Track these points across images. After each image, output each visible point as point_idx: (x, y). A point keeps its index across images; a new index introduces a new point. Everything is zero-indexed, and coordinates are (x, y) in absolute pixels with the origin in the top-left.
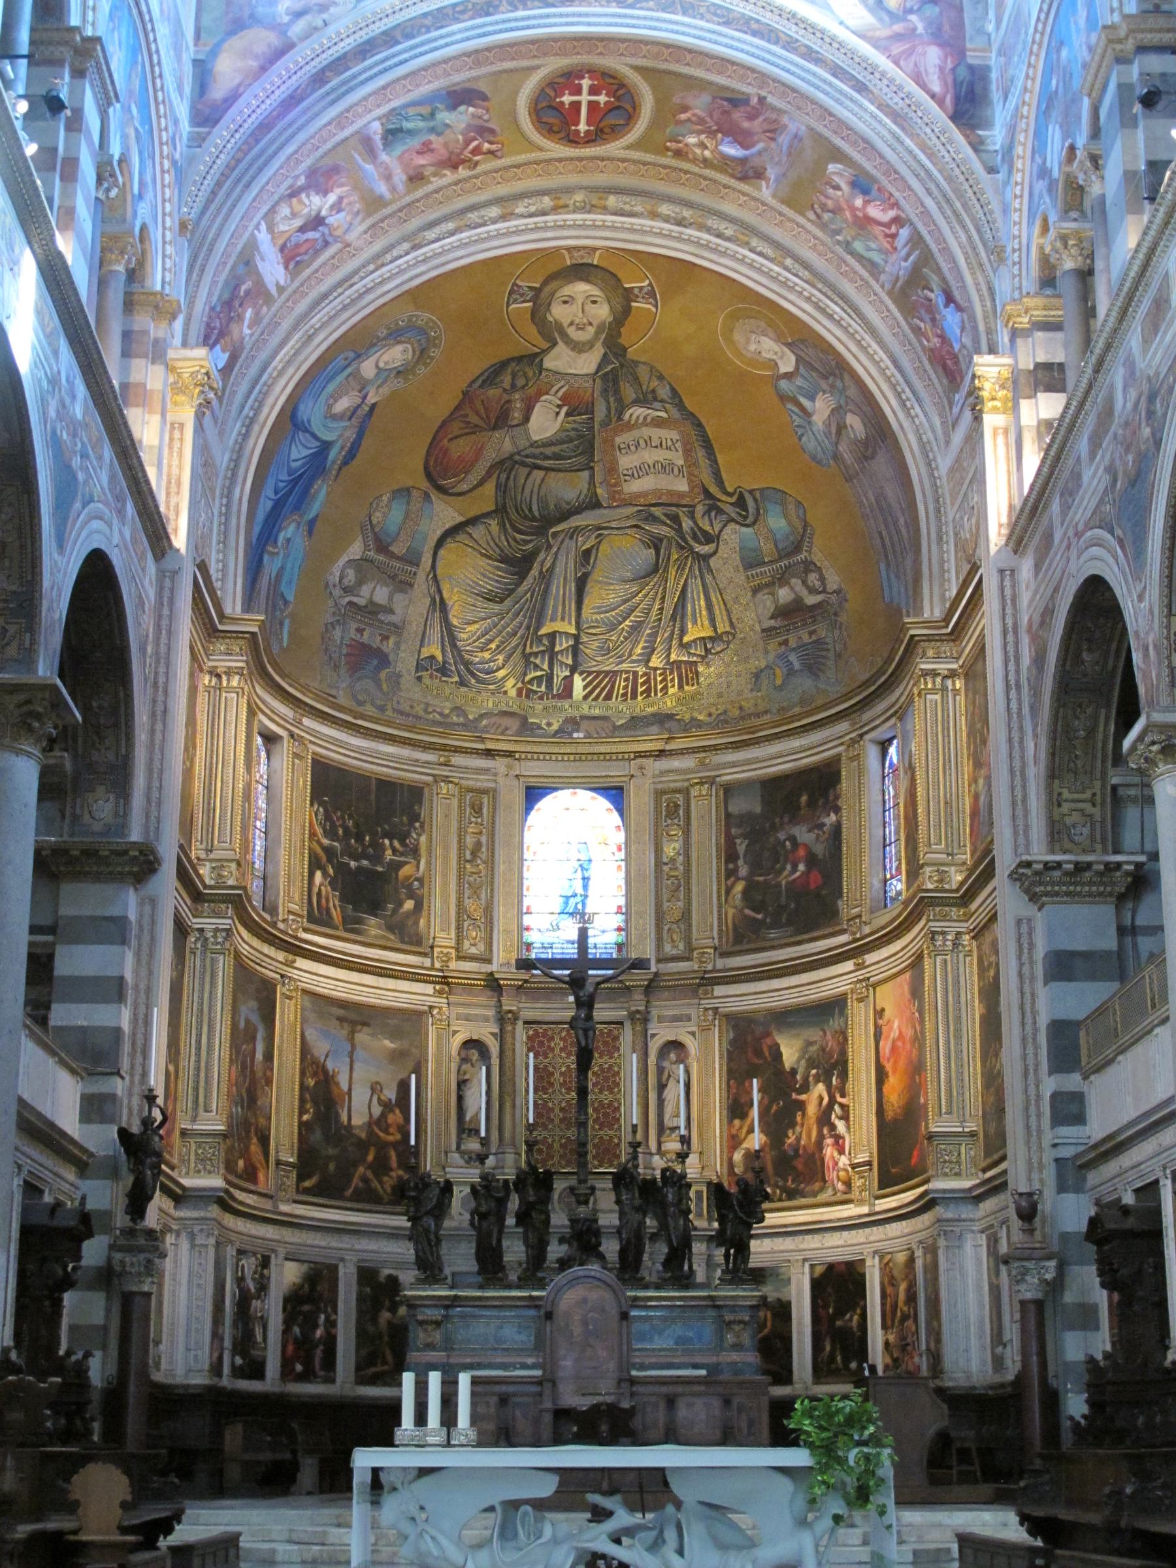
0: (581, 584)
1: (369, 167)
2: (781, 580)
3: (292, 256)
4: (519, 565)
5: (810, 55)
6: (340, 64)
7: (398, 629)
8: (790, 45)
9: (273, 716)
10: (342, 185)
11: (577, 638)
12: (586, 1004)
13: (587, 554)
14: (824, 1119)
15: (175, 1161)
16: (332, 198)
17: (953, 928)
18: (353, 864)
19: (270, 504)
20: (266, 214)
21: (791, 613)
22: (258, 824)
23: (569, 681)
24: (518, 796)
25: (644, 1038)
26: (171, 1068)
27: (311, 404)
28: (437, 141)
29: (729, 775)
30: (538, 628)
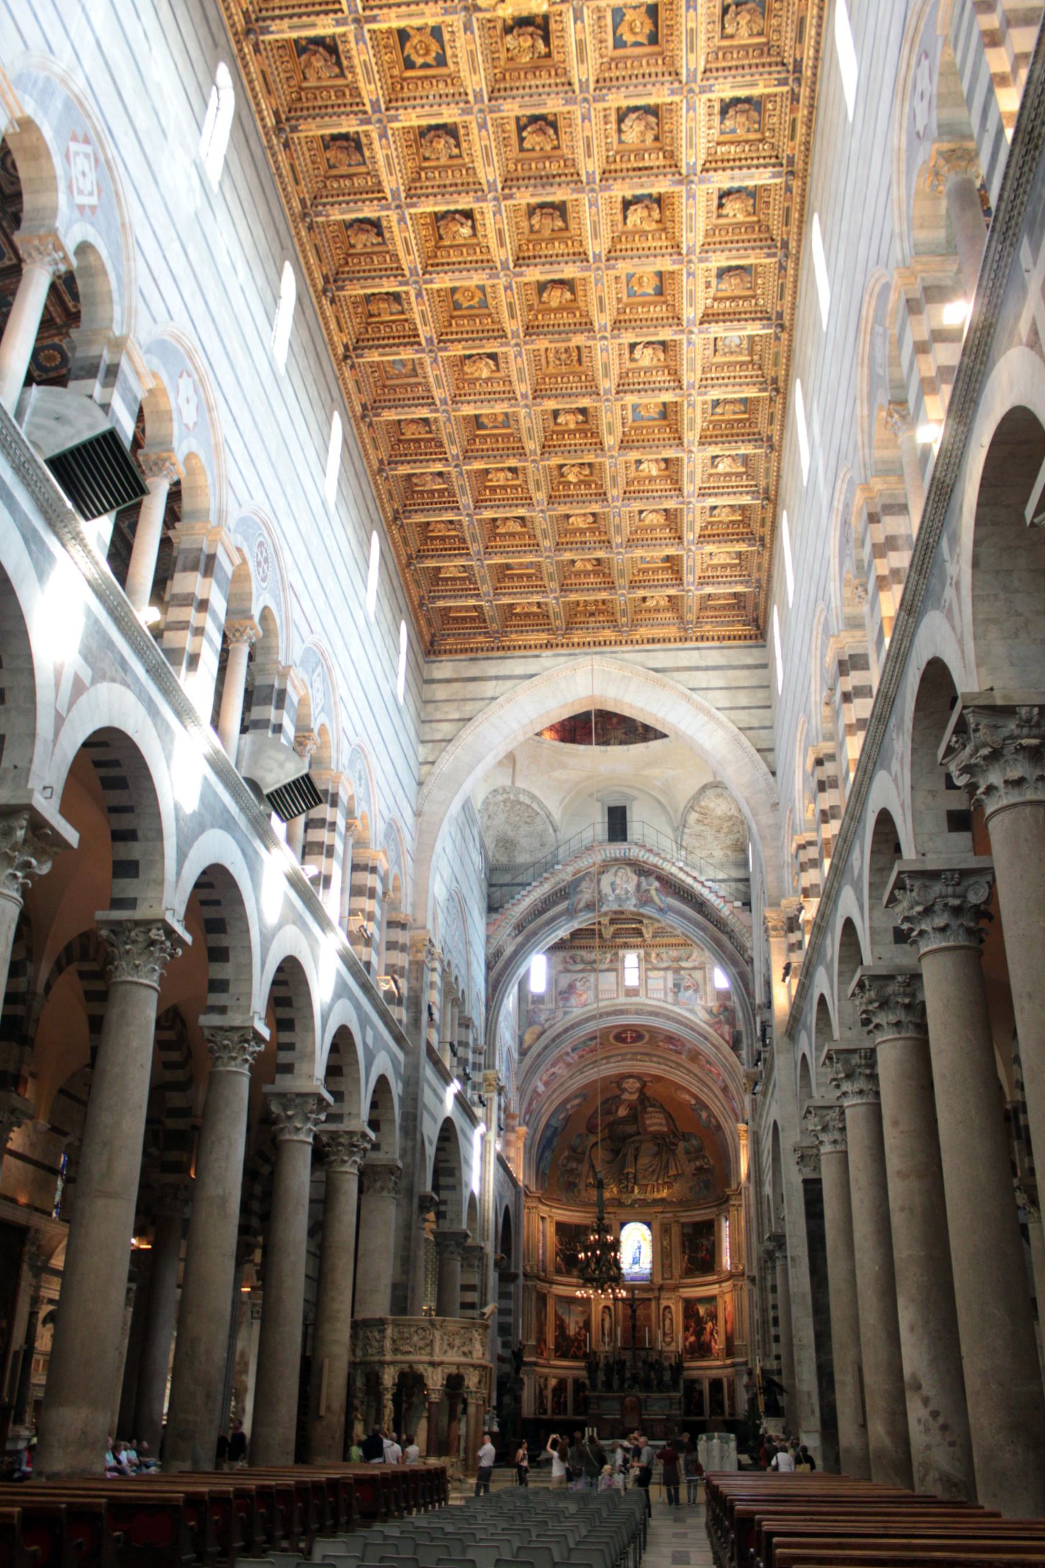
0: (636, 1158)
2: (697, 1158)
3: (546, 1084)
4: (616, 1152)
5: (692, 1029)
6: (559, 1035)
7: (579, 1175)
8: (686, 1025)
12: (634, 1311)
13: (637, 1149)
14: (711, 1334)
17: (740, 1283)
21: (700, 1169)
24: (618, 1225)
25: (659, 1304)
29: (683, 1220)
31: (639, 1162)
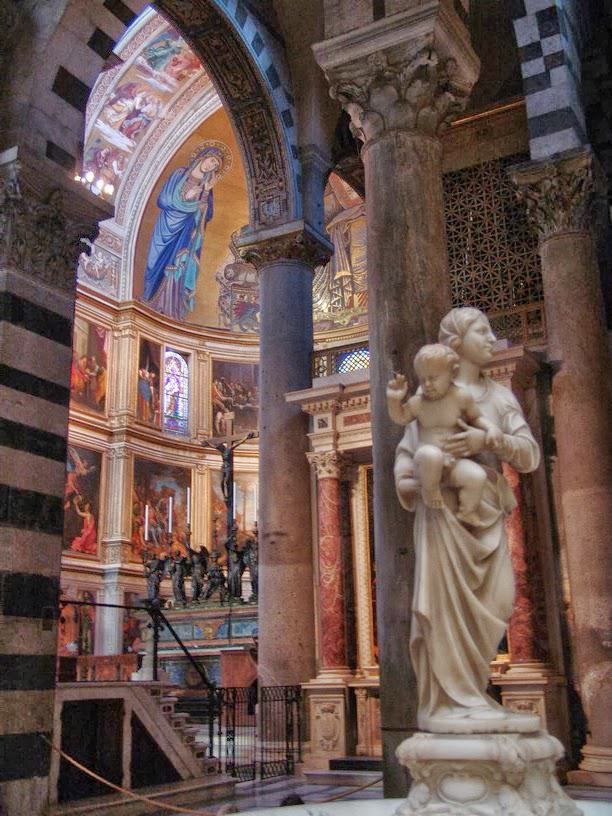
0: (348, 250)
1: (151, 80)
3: (128, 132)
9: (179, 344)
10: (140, 92)
11: (352, 277)
13: (346, 235)
15: (99, 558)
16: (138, 99)
18: (241, 407)
19: (161, 249)
20: (98, 117)
22: (181, 395)
23: (351, 299)
26: (88, 516)
27: (170, 198)
28: (180, 57)
30: (334, 275)
31: (353, 258)
